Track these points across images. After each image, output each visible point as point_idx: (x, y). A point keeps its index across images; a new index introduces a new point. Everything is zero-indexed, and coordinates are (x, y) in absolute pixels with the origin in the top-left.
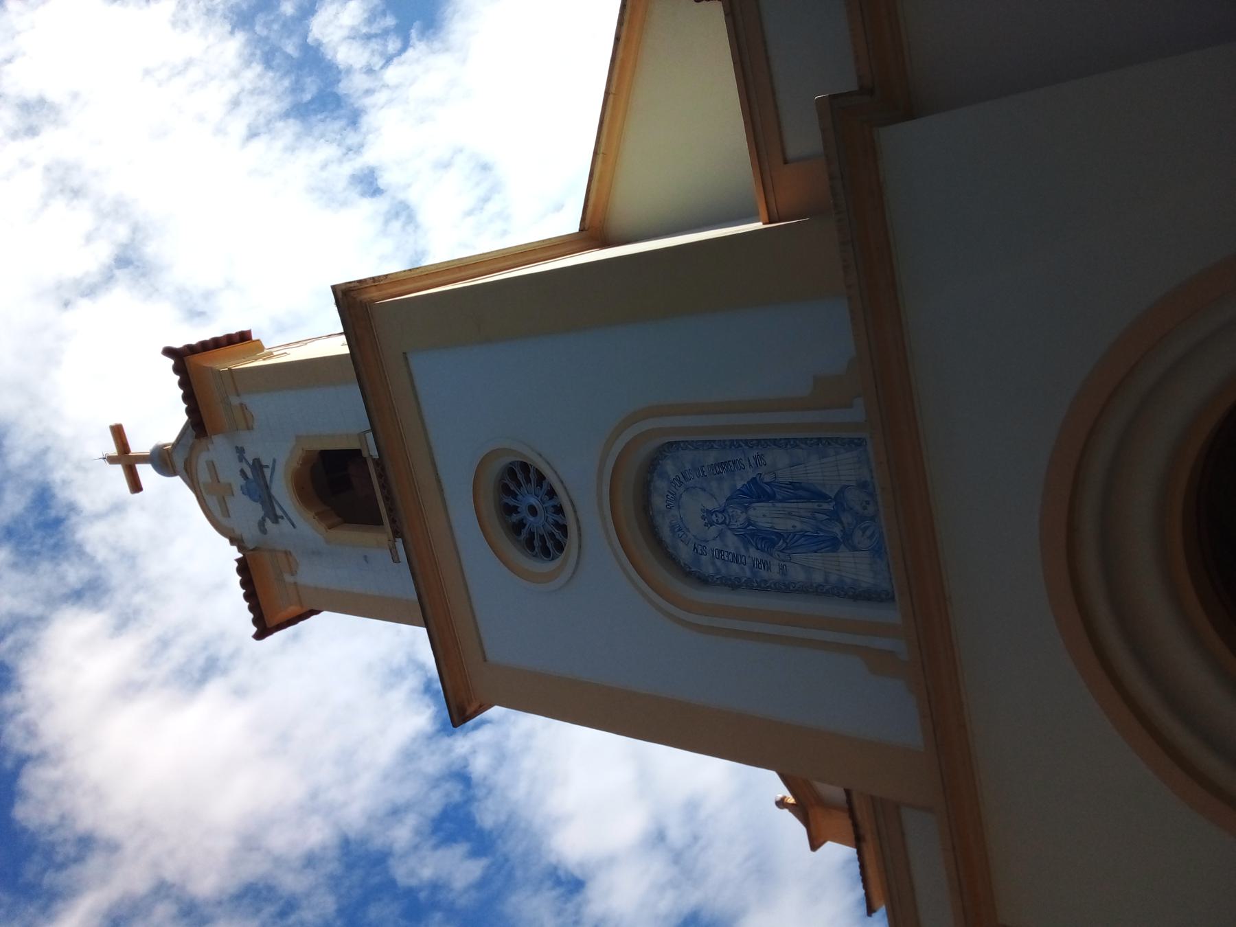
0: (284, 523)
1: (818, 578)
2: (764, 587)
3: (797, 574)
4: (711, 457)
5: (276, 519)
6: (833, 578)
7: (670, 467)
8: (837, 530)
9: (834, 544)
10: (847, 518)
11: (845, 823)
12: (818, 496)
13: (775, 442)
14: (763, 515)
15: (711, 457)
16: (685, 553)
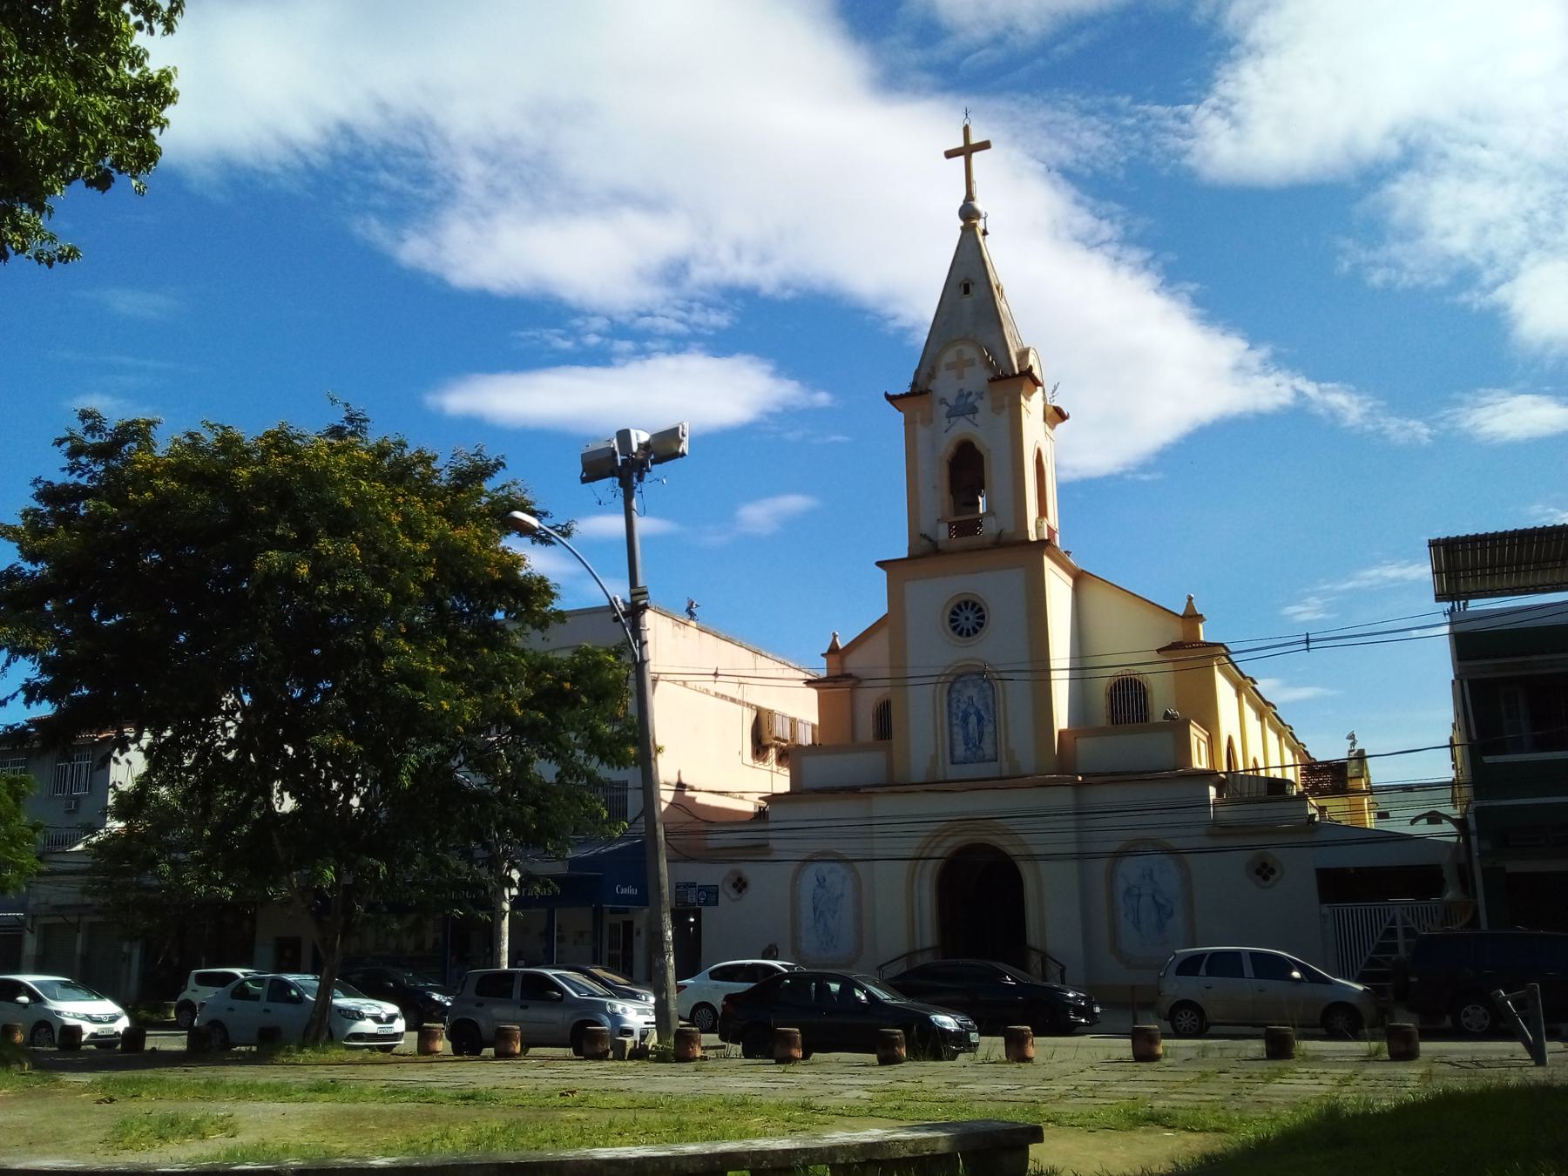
0: (945, 423)
1: (955, 737)
2: (950, 717)
3: (956, 729)
4: (990, 703)
5: (949, 416)
8: (970, 746)
9: (966, 744)
10: (974, 749)
11: (838, 673)
13: (995, 728)
14: (973, 719)
15: (990, 703)
16: (958, 686)
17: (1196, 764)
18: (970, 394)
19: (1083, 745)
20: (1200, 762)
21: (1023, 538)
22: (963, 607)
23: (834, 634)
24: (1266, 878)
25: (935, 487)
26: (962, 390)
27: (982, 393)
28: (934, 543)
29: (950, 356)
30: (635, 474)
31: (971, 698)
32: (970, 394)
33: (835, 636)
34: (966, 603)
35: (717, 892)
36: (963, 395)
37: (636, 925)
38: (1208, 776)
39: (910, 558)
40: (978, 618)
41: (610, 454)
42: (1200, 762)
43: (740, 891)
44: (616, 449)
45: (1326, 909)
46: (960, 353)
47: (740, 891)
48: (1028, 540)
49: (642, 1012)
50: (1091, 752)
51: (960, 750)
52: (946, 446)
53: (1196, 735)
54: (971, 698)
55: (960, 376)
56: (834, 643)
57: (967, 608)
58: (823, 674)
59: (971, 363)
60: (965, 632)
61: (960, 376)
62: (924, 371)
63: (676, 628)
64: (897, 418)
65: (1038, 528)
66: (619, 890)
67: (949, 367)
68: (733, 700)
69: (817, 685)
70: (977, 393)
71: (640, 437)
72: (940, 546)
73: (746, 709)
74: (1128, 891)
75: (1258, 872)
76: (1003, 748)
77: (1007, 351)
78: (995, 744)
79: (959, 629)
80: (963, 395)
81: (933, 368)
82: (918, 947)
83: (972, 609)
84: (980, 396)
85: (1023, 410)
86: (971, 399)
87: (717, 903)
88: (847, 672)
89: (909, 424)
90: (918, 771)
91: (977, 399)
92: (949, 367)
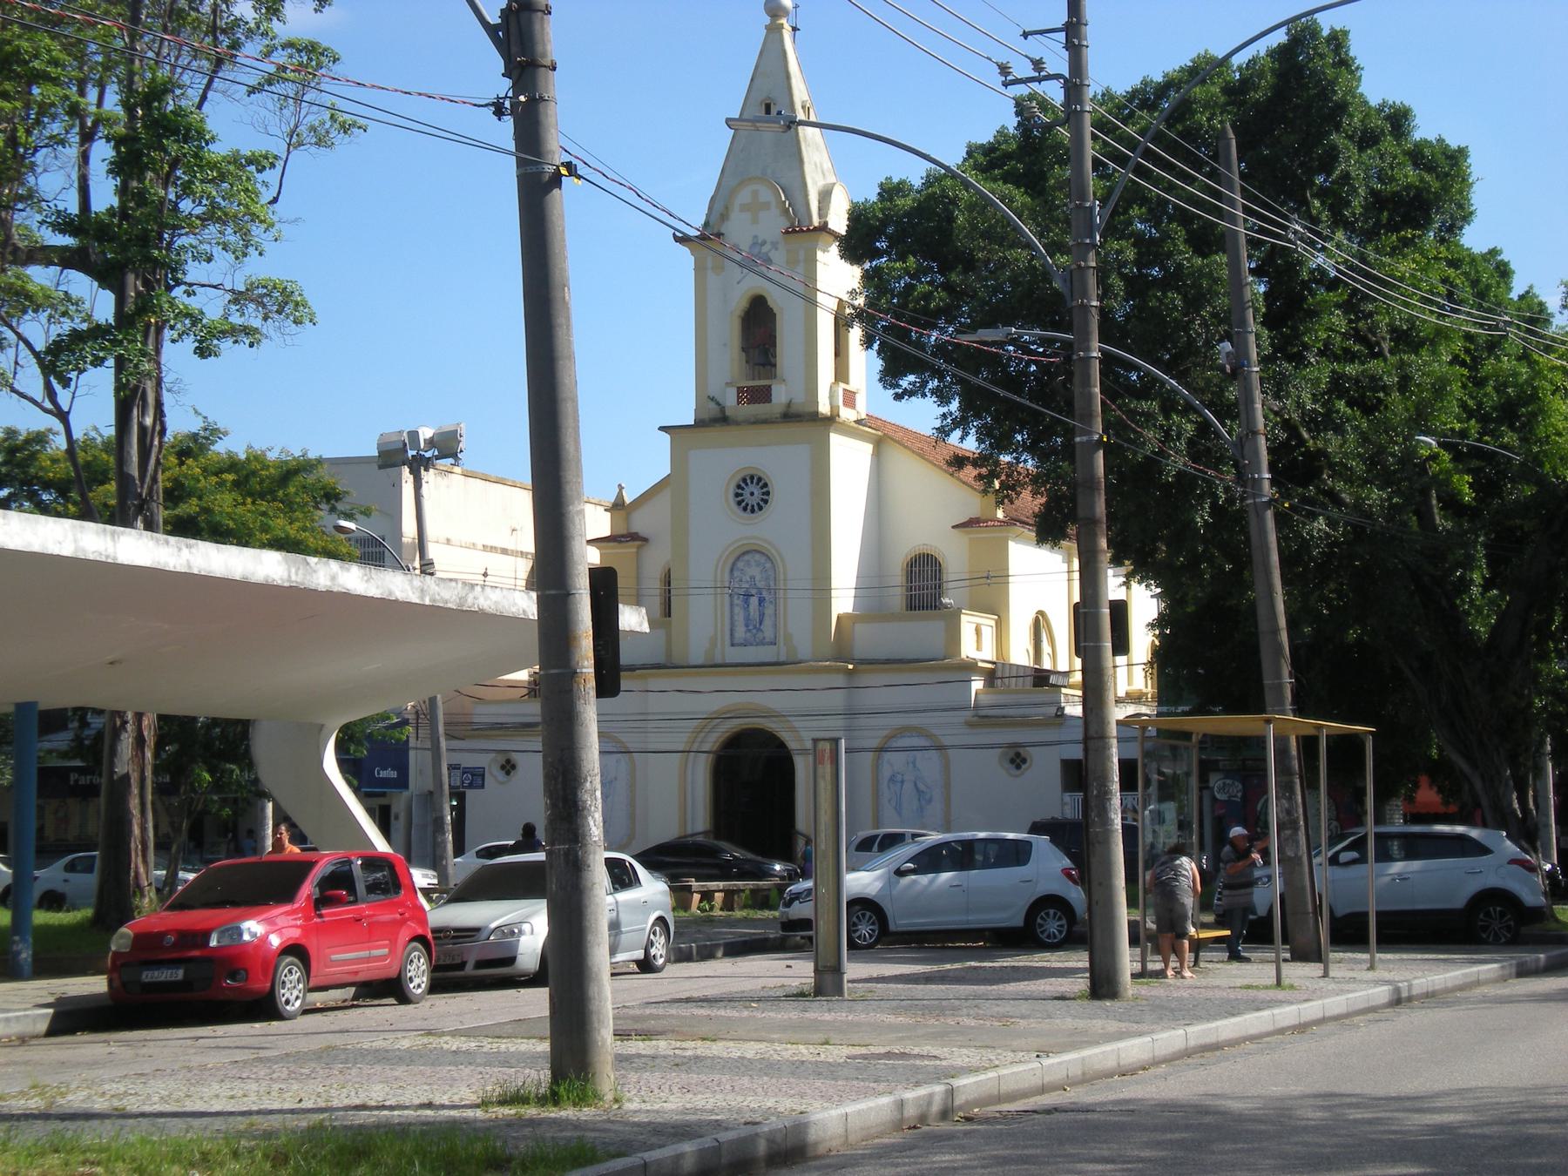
1: (736, 618)
3: (737, 610)
6: (737, 623)
7: (768, 565)
8: (751, 627)
9: (747, 626)
10: (754, 631)
12: (760, 624)
14: (754, 601)
16: (740, 565)
17: (968, 649)
18: (764, 243)
19: (861, 630)
20: (979, 648)
21: (811, 410)
22: (749, 481)
23: (620, 485)
24: (1018, 767)
25: (725, 345)
26: (756, 237)
27: (777, 243)
28: (723, 409)
29: (744, 196)
30: (422, 468)
31: (752, 578)
32: (764, 243)
33: (621, 488)
34: (752, 478)
35: (483, 775)
36: (757, 243)
37: (394, 810)
38: (970, 667)
39: (700, 423)
40: (763, 494)
41: (401, 446)
42: (979, 648)
43: (508, 773)
44: (407, 441)
45: (1067, 797)
46: (755, 194)
47: (508, 773)
48: (817, 413)
49: (425, 876)
50: (868, 641)
51: (740, 632)
52: (739, 302)
53: (968, 622)
54: (752, 578)
55: (755, 221)
56: (620, 496)
57: (752, 482)
58: (606, 532)
59: (766, 206)
60: (749, 507)
61: (755, 221)
62: (718, 207)
63: (439, 478)
64: (685, 258)
65: (832, 396)
66: (379, 774)
67: (745, 208)
68: (504, 551)
69: (599, 544)
70: (772, 243)
71: (426, 433)
72: (728, 413)
73: (519, 559)
74: (892, 779)
75: (1012, 761)
76: (782, 633)
77: (806, 195)
78: (775, 626)
79: (743, 504)
80: (757, 243)
81: (727, 208)
82: (689, 831)
83: (758, 484)
84: (775, 245)
85: (819, 266)
86: (765, 249)
87: (482, 786)
88: (634, 530)
89: (700, 270)
90: (697, 657)
91: (770, 250)
92: (745, 208)
